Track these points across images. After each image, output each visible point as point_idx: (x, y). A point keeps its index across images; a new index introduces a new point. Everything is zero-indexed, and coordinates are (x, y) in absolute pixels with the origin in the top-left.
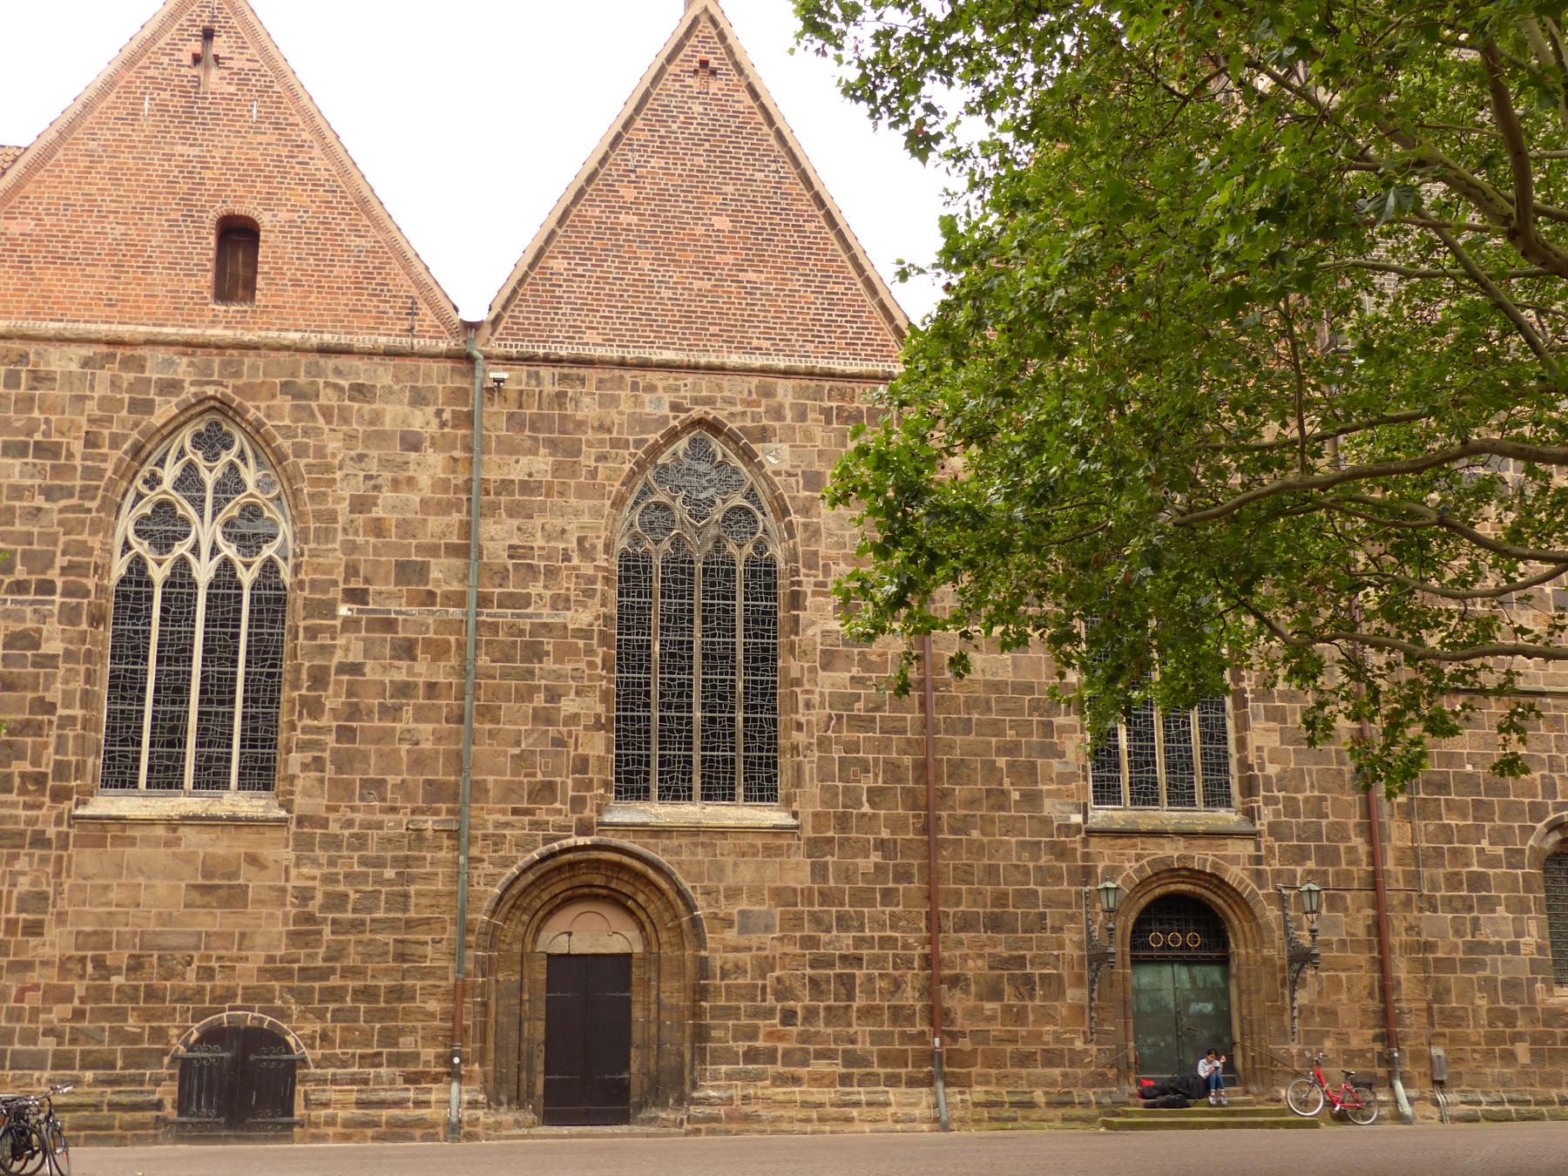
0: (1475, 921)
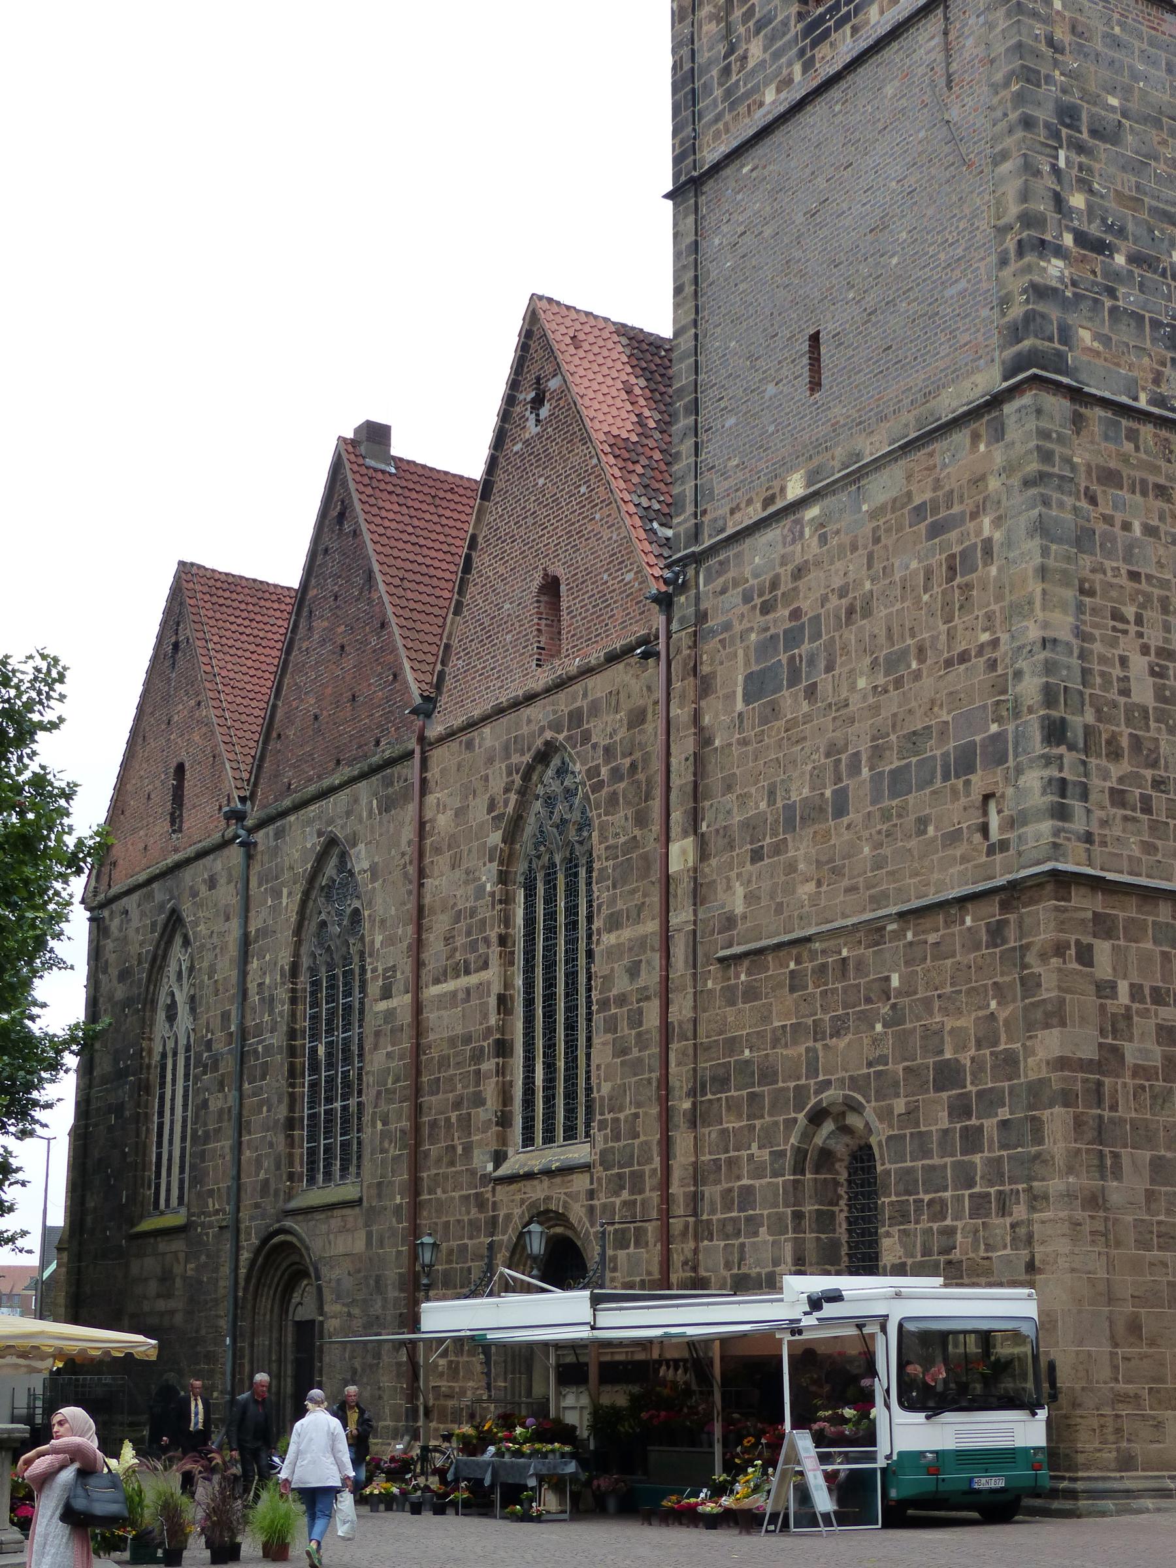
0: (743, 1245)
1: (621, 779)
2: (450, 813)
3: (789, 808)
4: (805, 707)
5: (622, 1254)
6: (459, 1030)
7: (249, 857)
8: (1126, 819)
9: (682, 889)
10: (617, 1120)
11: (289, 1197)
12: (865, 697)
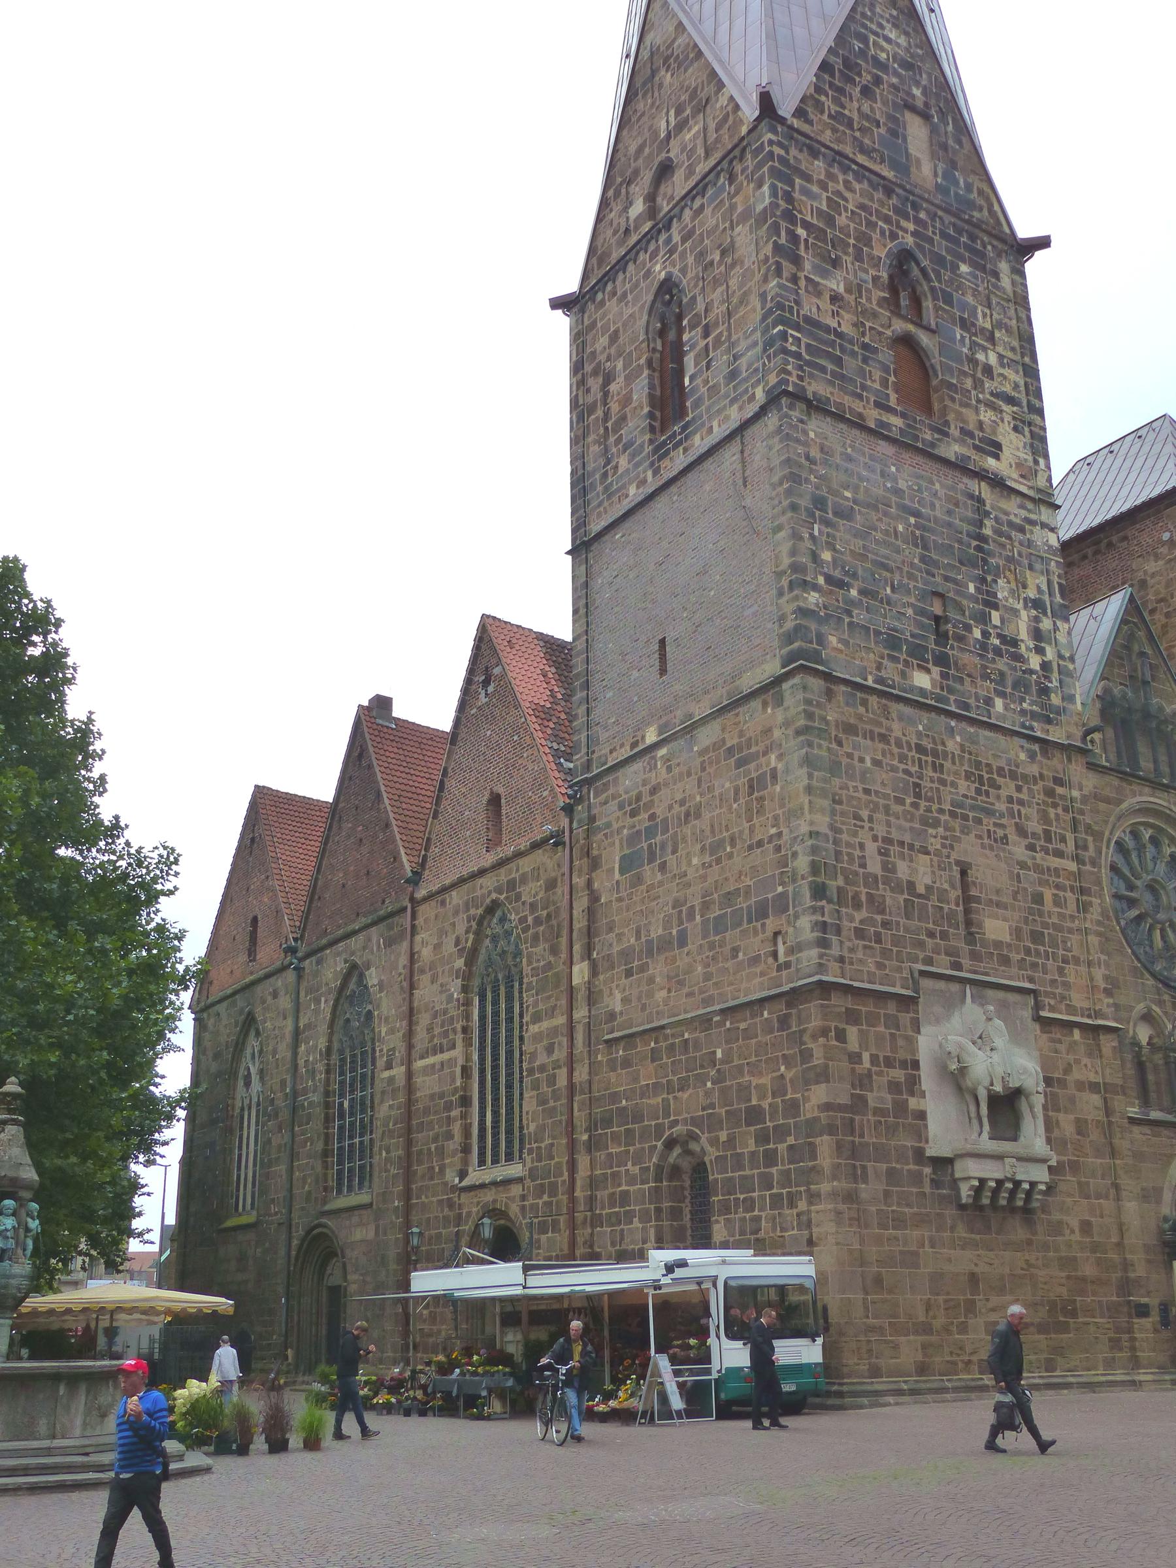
0: (622, 1230)
1: (541, 924)
2: (430, 947)
3: (649, 942)
4: (659, 877)
5: (543, 1237)
6: (436, 1089)
7: (300, 977)
8: (865, 947)
9: (581, 996)
10: (539, 1148)
11: (325, 1203)
12: (697, 870)
